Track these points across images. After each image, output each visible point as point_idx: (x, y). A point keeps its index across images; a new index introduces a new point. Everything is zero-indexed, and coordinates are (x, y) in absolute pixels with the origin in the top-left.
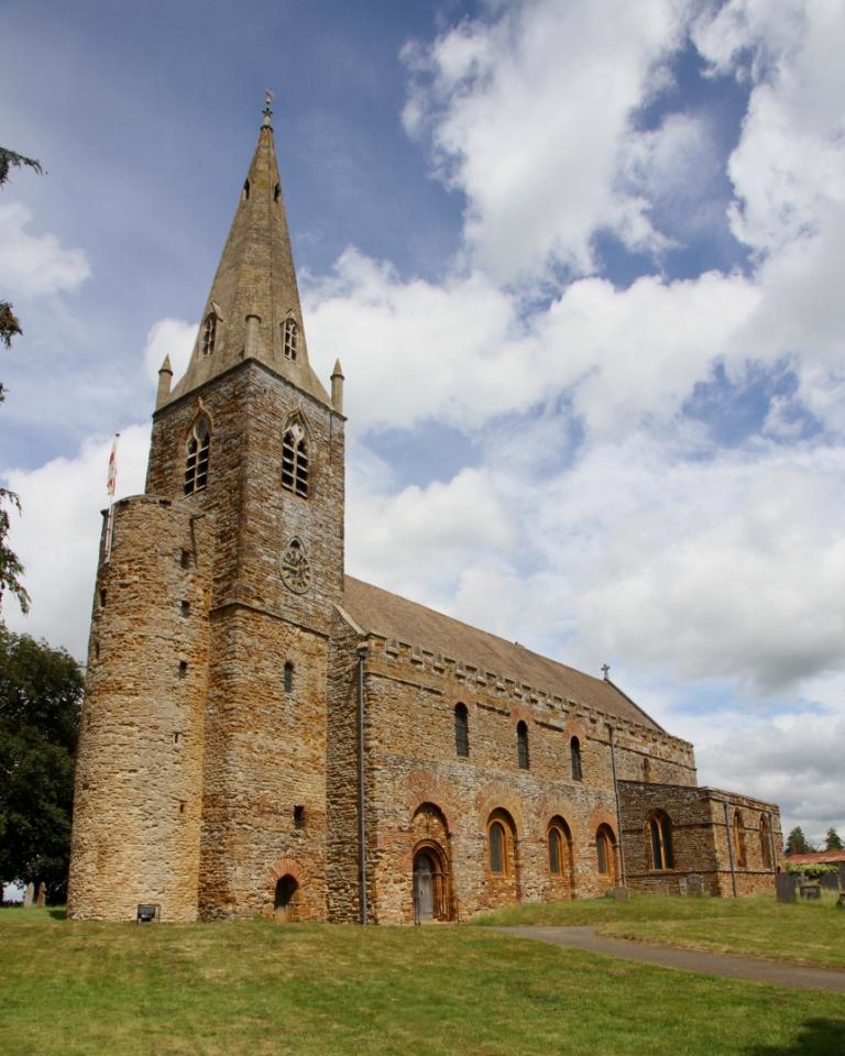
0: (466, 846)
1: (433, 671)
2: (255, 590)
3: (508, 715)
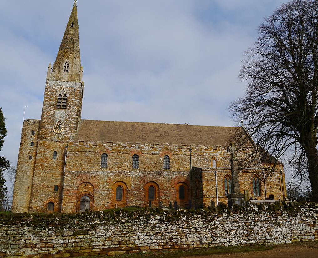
0: (101, 193)
1: (93, 146)
2: (44, 136)
3: (128, 153)
